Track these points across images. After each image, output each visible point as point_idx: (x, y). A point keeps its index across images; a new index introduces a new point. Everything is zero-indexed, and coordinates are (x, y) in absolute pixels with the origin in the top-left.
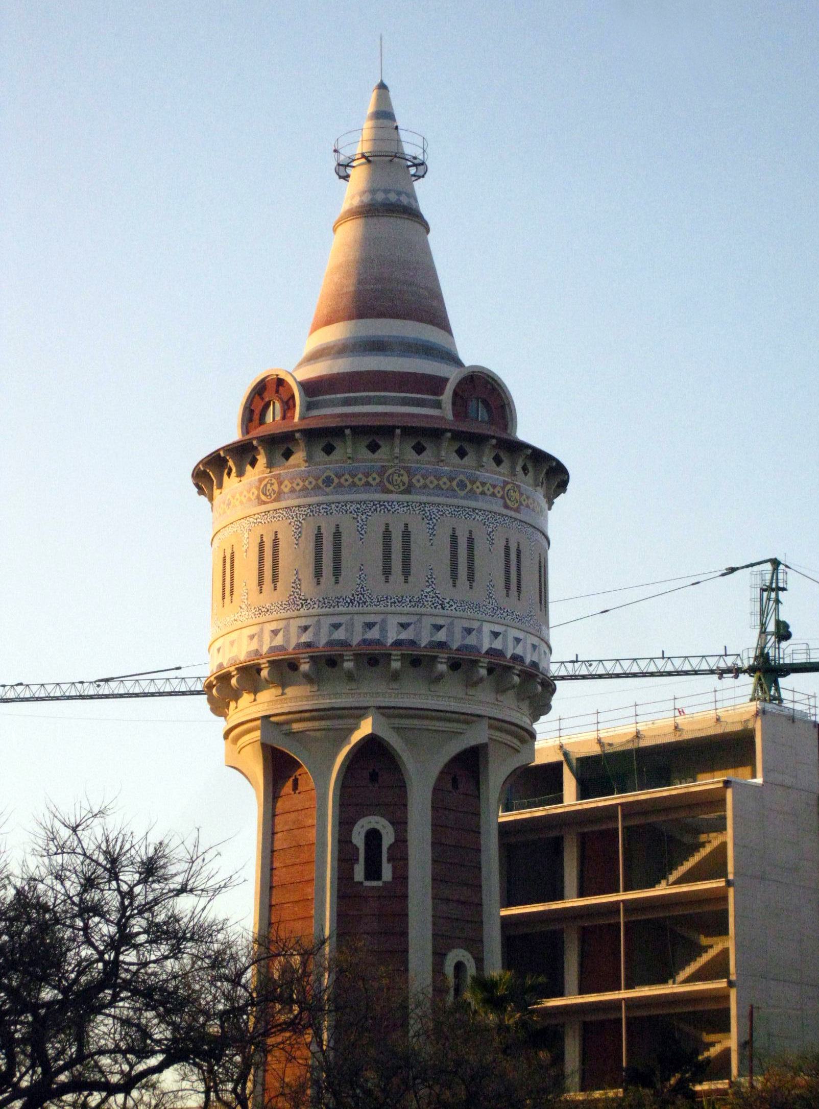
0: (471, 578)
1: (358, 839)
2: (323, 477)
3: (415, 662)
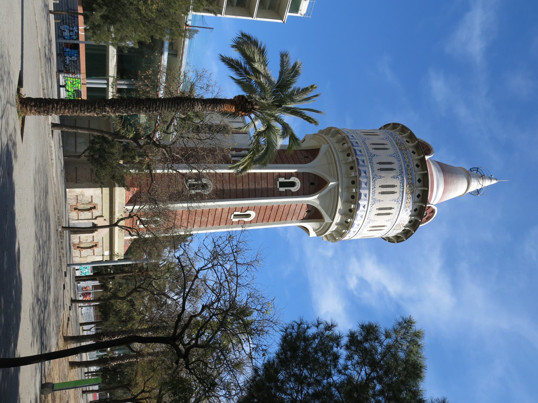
0: (378, 214)
1: (292, 179)
3: (353, 197)
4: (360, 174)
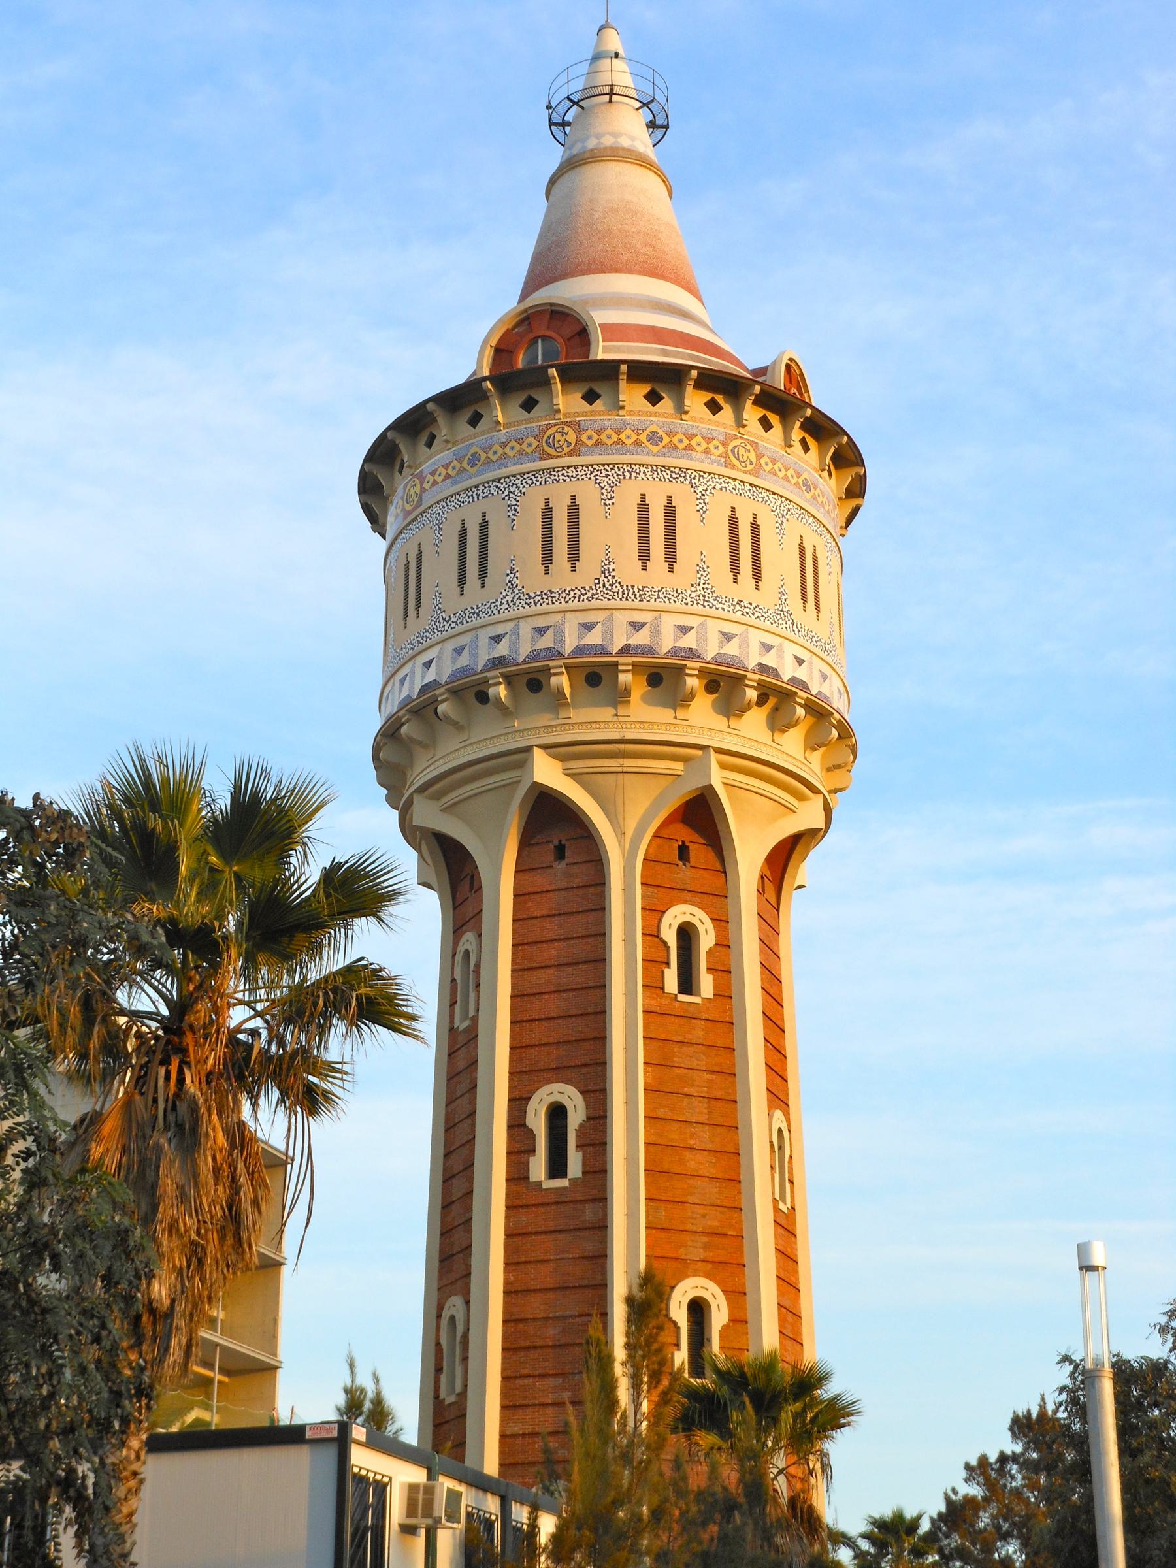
1: (670, 936)
2: (648, 432)
4: (692, 654)
